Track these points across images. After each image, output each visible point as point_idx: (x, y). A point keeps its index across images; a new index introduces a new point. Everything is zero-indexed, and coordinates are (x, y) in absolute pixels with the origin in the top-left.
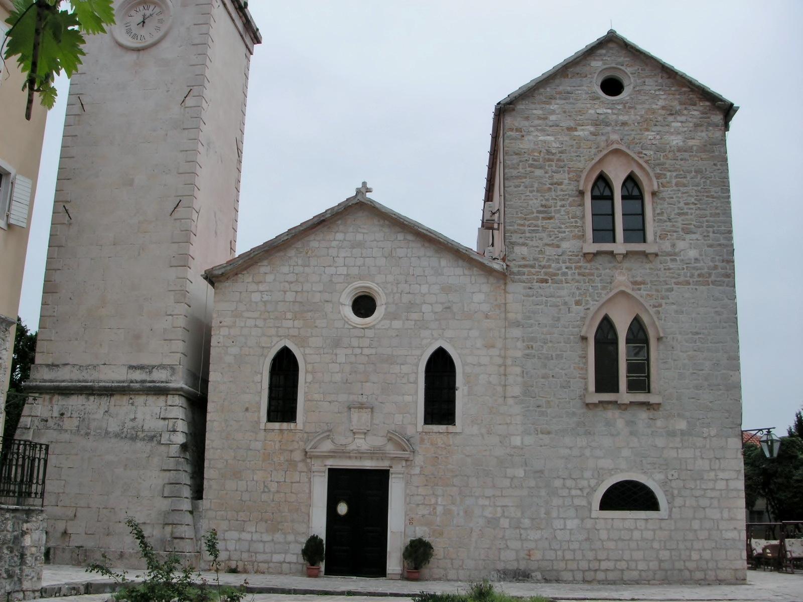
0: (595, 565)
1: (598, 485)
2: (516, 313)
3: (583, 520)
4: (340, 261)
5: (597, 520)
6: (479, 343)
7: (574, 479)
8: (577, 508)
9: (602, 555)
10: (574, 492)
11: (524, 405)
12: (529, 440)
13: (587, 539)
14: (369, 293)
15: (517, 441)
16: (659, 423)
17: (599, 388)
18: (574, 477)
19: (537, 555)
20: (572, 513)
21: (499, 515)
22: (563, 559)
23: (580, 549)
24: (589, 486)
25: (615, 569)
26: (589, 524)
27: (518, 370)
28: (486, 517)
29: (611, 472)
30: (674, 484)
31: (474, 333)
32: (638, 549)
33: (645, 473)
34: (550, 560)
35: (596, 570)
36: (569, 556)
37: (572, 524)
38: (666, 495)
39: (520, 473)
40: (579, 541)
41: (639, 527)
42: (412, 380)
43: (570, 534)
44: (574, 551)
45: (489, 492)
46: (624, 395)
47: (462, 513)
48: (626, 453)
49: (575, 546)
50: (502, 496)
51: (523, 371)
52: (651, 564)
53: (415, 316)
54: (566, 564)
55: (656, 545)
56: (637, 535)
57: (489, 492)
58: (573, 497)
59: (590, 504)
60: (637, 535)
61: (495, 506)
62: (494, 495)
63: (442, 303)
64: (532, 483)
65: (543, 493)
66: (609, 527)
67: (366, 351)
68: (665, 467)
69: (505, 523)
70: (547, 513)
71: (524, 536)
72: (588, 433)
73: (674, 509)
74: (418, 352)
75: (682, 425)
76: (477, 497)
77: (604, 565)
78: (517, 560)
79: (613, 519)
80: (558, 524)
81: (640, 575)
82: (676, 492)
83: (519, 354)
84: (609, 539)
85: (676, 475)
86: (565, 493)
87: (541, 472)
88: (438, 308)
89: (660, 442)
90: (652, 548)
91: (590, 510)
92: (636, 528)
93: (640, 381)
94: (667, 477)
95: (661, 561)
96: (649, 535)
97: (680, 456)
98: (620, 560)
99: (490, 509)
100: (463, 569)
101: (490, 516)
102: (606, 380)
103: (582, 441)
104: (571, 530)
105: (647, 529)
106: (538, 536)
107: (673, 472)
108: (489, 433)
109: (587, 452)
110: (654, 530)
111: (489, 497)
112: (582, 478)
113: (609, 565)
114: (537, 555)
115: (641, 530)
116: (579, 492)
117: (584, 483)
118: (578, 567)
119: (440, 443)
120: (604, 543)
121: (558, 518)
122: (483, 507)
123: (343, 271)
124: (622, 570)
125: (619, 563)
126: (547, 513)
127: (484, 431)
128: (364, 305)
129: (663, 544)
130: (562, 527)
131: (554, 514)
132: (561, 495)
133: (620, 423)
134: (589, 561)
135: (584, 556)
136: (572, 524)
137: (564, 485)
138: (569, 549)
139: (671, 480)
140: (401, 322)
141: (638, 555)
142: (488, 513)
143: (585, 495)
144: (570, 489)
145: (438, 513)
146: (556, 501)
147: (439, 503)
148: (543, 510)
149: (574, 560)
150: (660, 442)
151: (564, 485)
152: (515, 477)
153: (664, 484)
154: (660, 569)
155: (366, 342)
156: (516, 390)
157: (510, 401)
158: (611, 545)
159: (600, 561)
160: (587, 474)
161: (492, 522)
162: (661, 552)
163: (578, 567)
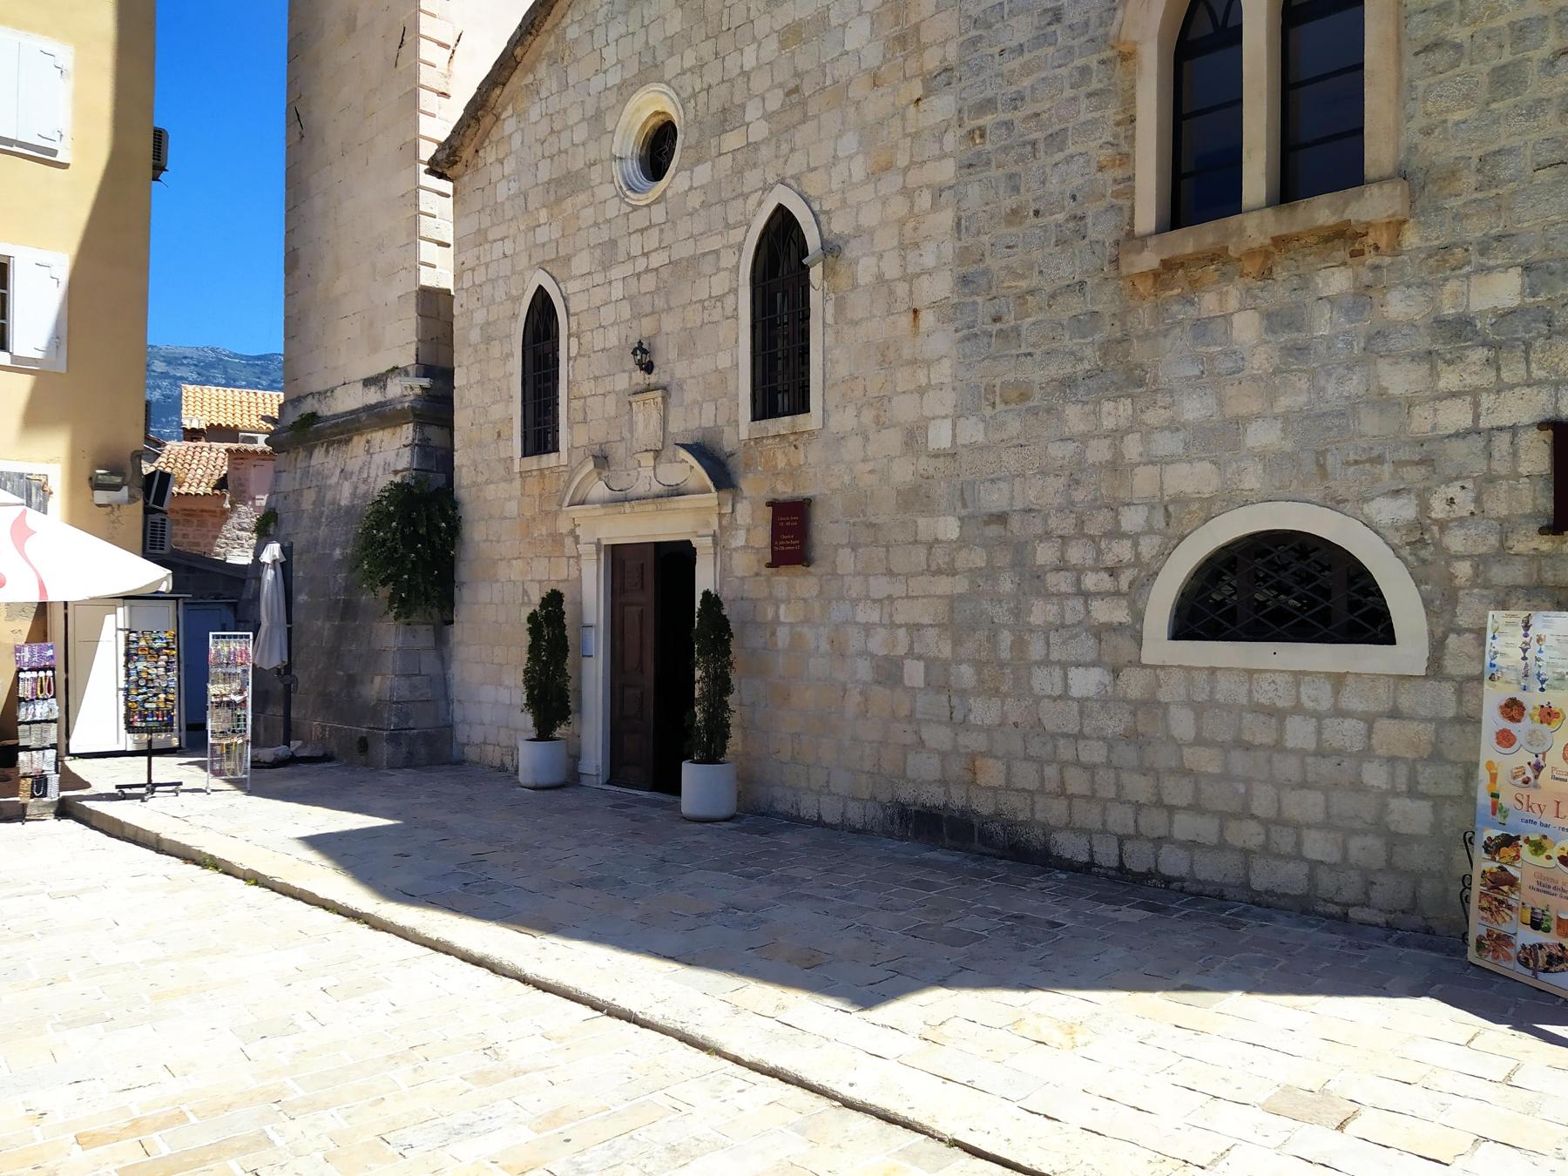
0: (1154, 822)
1: (1165, 554)
2: (944, 44)
3: (1116, 672)
4: (610, 54)
5: (1161, 674)
6: (858, 170)
7: (1092, 538)
8: (1100, 632)
9: (1178, 792)
10: (1090, 581)
11: (958, 324)
12: (972, 431)
13: (1132, 737)
14: (657, 113)
15: (940, 437)
16: (1399, 306)
17: (1177, 215)
18: (1092, 529)
19: (992, 773)
20: (1085, 647)
21: (901, 650)
22: (1062, 793)
23: (1109, 764)
24: (1138, 555)
25: (1222, 846)
26: (1134, 684)
27: (946, 218)
28: (873, 656)
29: (1209, 510)
30: (1455, 541)
31: (849, 143)
32: (1304, 785)
33: (1334, 503)
34: (1024, 790)
35: (1159, 841)
36: (1077, 783)
37: (1086, 682)
38: (1419, 582)
39: (949, 528)
40: (1104, 739)
41: (1308, 704)
42: (729, 312)
43: (1081, 713)
44: (1091, 768)
45: (880, 586)
46: (1256, 222)
47: (825, 646)
48: (1263, 436)
49: (1094, 753)
50: (907, 597)
51: (960, 219)
52: (1355, 844)
53: (733, 140)
54: (1070, 807)
55: (1375, 776)
56: (1299, 733)
57: (880, 586)
58: (1086, 595)
59: (1139, 616)
60: (1299, 733)
61: (894, 626)
62: (890, 597)
63: (780, 85)
64: (978, 558)
65: (1007, 585)
66: (1202, 697)
67: (658, 259)
68: (1414, 474)
69: (914, 673)
70: (1020, 644)
71: (958, 716)
72: (1133, 381)
73: (1452, 640)
74: (736, 235)
75: (1502, 290)
76: (855, 602)
77: (1186, 826)
78: (944, 782)
79: (1213, 671)
80: (1045, 681)
81: (1311, 877)
82: (1463, 569)
83: (946, 171)
84: (1199, 741)
85: (1465, 504)
86: (1060, 582)
87: (1001, 518)
88: (775, 102)
89: (1399, 379)
90: (1358, 787)
91: (1138, 639)
92: (1298, 709)
93: (1323, 150)
94: (1424, 507)
95: (1394, 840)
96: (1347, 734)
97: (1484, 423)
98: (1236, 816)
99: (881, 631)
100: (830, 794)
101: (882, 652)
102: (1200, 183)
103: (1115, 413)
104: (1082, 701)
105: (1340, 713)
106: (992, 717)
107: (1453, 490)
108: (880, 424)
109: (1132, 448)
110: (1370, 720)
111: (880, 601)
112: (1116, 534)
113: (1205, 829)
114: (992, 773)
115: (1318, 716)
116: (1106, 582)
117: (1121, 551)
118: (1104, 823)
119: (781, 463)
120: (1186, 751)
121: (1046, 662)
122: (868, 628)
123: (614, 78)
124: (1246, 853)
125: (1233, 825)
126: (1020, 644)
127: (868, 416)
128: (658, 150)
129: (1402, 771)
130: (1057, 692)
131: (1036, 650)
132: (1054, 590)
133: (1246, 327)
134: (1138, 807)
135: (1119, 787)
136: (1086, 682)
137: (1062, 559)
138: (1077, 763)
139: (1443, 525)
140: (709, 164)
141: (1308, 806)
142: (877, 645)
143: (1124, 586)
144: (1079, 571)
145: (780, 644)
146: (1041, 611)
147: (782, 619)
148: (1006, 638)
149: (1091, 798)
150: (1399, 379)
151: (1062, 559)
152: (937, 540)
153: (1418, 543)
154: (1390, 867)
155: (652, 239)
156: (939, 287)
157: (927, 318)
158: (1206, 761)
159: (1172, 810)
160: (1132, 519)
161: (889, 672)
162: (1395, 804)
163: (1104, 823)
